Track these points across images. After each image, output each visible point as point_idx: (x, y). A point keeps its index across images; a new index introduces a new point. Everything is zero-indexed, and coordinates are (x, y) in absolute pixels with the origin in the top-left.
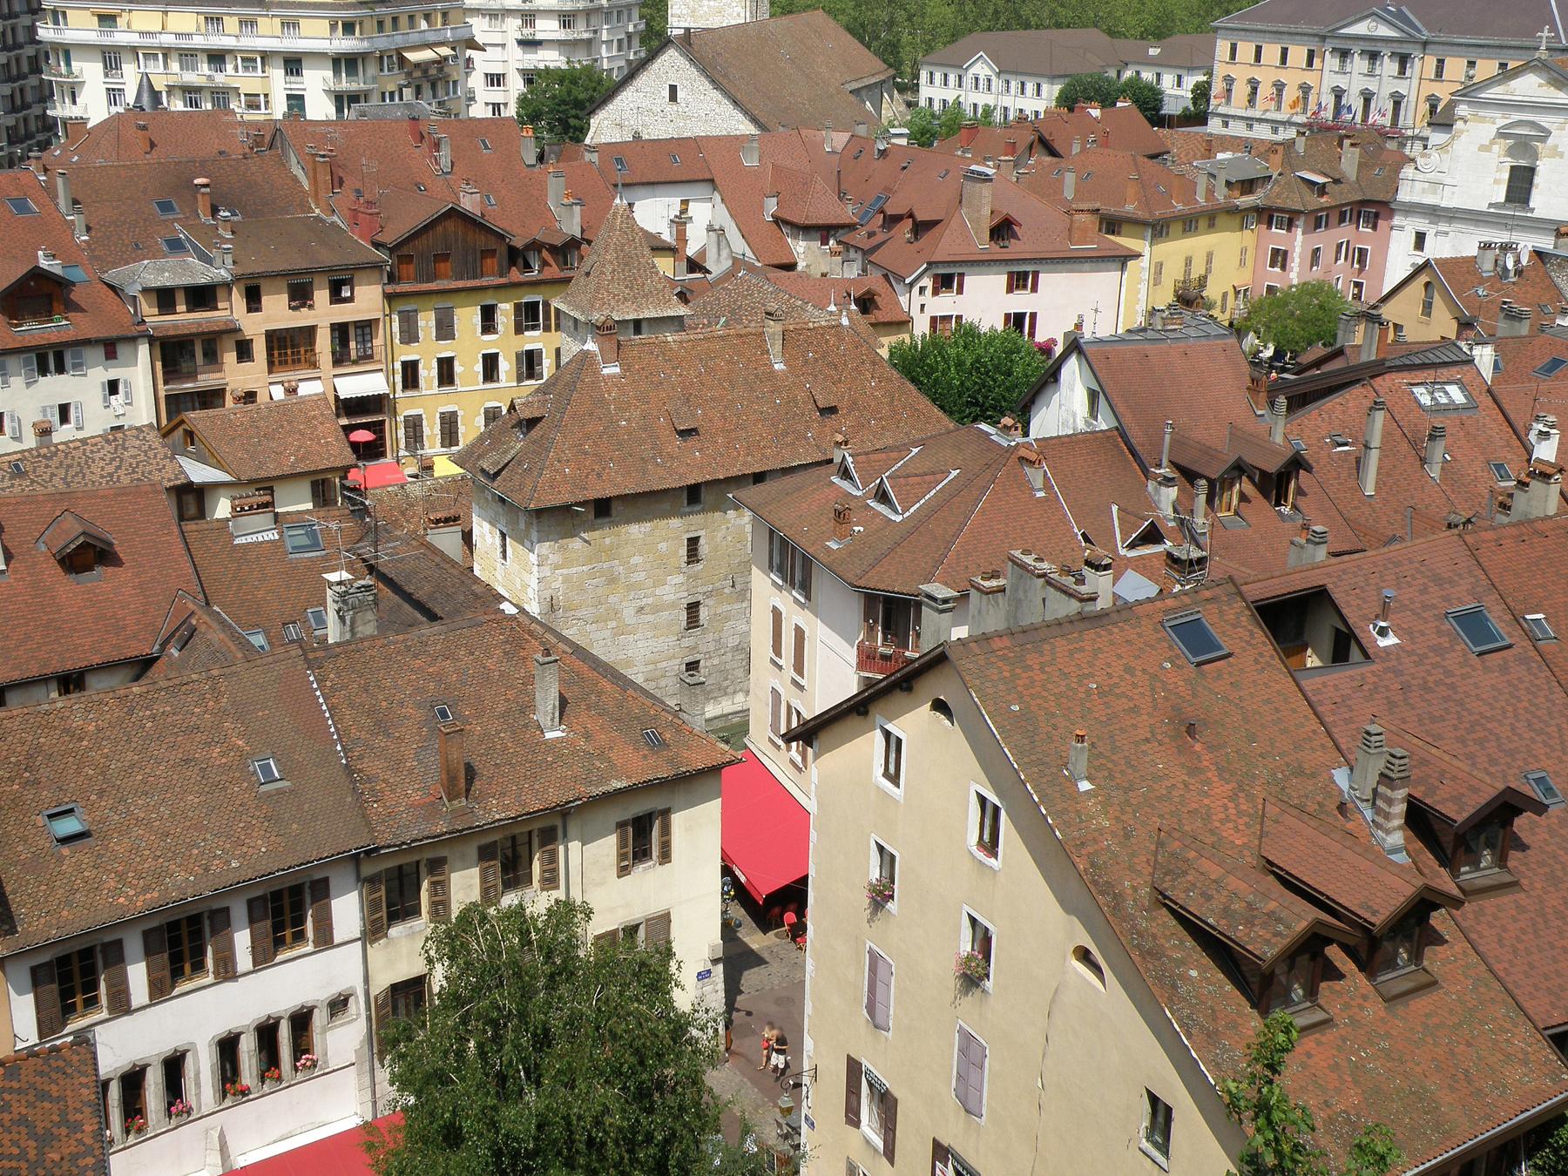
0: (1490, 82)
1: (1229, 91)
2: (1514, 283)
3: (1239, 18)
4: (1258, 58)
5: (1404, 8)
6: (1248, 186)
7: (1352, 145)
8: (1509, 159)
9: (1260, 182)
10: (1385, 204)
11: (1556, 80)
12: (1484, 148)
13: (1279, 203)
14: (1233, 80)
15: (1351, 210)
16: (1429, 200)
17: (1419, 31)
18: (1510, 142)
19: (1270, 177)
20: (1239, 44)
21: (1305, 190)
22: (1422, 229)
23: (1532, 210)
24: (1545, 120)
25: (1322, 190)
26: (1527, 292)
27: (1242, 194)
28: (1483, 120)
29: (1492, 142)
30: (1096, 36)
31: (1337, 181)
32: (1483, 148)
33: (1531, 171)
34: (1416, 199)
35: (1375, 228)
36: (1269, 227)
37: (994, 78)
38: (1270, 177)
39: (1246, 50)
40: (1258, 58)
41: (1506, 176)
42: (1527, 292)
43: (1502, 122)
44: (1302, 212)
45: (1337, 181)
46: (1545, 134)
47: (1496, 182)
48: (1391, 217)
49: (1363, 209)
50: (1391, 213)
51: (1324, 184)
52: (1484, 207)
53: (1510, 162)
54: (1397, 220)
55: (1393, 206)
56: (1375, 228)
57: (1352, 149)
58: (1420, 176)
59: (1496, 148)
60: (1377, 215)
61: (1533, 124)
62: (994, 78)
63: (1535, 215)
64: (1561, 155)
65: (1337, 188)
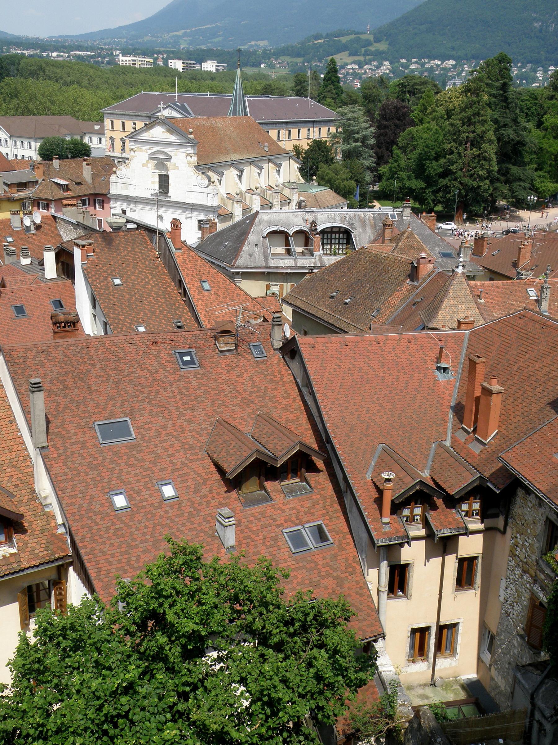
0: (142, 131)
1: (113, 144)
2: (33, 234)
3: (114, 108)
4: (123, 128)
5: (185, 104)
6: (22, 186)
7: (87, 164)
8: (157, 171)
9: (30, 184)
10: (105, 195)
11: (169, 130)
12: (144, 165)
13: (41, 196)
14: (114, 139)
15: (89, 199)
16: (125, 193)
17: (190, 114)
18: (155, 162)
19: (37, 182)
20: (115, 121)
21: (55, 188)
22: (124, 208)
23: (170, 197)
24: (168, 150)
25: (66, 188)
26: (41, 239)
27: (18, 191)
28: (141, 150)
29: (148, 162)
30: (69, 120)
31: (78, 184)
32: (144, 165)
33: (167, 176)
34: (119, 192)
35: (103, 208)
36: (39, 209)
37: (8, 139)
38: (37, 182)
39: (118, 124)
40: (123, 128)
41: (157, 179)
42: (41, 239)
43: (150, 151)
44: (51, 200)
45: (78, 184)
46: (169, 158)
47: (153, 183)
48: (109, 202)
49: (97, 199)
50: (109, 200)
51: (67, 185)
52: (149, 196)
53: (158, 172)
54: (112, 204)
55: (109, 196)
56: (103, 208)
57: (87, 167)
58: (119, 180)
59: (149, 165)
60: (103, 201)
61: (163, 152)
62: (8, 139)
63: (172, 199)
64: (178, 168)
65: (78, 187)
